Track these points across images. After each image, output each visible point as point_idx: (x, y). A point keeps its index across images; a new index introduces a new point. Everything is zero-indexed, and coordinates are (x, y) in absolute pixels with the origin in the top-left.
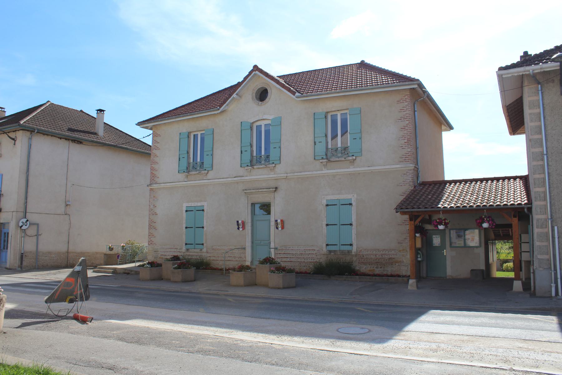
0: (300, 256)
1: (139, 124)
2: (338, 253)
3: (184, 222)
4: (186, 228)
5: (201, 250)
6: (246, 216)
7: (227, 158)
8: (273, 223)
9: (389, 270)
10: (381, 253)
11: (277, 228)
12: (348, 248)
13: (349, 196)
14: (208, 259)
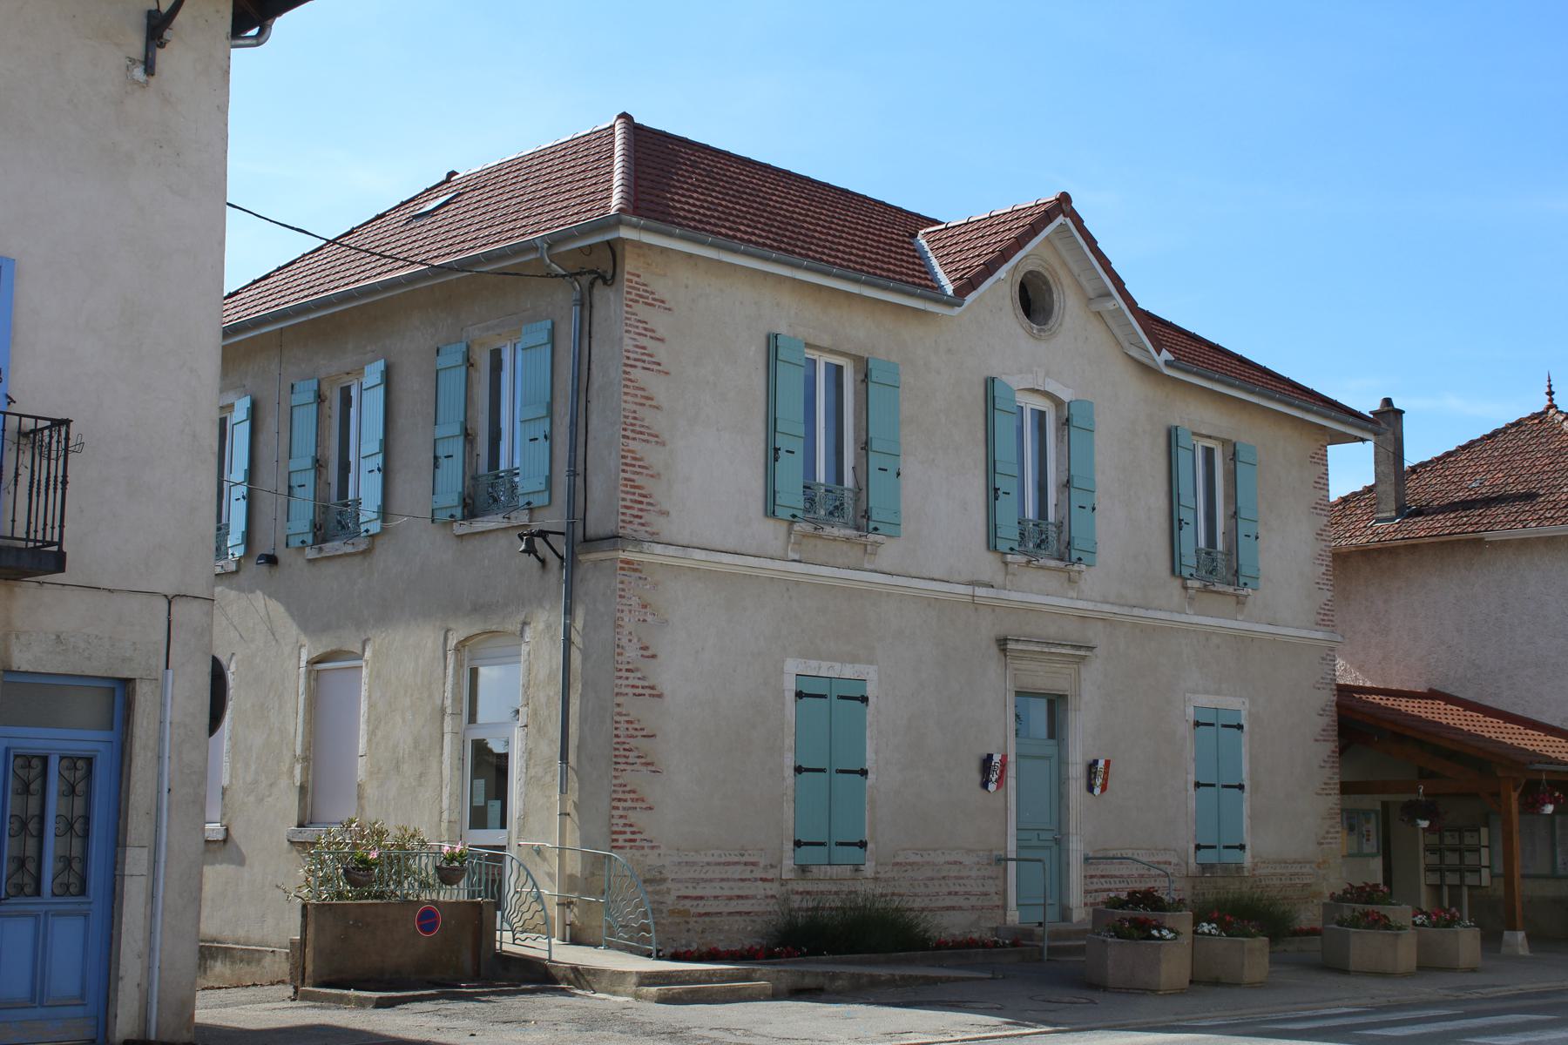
3: (789, 741)
5: (857, 868)
7: (940, 499)
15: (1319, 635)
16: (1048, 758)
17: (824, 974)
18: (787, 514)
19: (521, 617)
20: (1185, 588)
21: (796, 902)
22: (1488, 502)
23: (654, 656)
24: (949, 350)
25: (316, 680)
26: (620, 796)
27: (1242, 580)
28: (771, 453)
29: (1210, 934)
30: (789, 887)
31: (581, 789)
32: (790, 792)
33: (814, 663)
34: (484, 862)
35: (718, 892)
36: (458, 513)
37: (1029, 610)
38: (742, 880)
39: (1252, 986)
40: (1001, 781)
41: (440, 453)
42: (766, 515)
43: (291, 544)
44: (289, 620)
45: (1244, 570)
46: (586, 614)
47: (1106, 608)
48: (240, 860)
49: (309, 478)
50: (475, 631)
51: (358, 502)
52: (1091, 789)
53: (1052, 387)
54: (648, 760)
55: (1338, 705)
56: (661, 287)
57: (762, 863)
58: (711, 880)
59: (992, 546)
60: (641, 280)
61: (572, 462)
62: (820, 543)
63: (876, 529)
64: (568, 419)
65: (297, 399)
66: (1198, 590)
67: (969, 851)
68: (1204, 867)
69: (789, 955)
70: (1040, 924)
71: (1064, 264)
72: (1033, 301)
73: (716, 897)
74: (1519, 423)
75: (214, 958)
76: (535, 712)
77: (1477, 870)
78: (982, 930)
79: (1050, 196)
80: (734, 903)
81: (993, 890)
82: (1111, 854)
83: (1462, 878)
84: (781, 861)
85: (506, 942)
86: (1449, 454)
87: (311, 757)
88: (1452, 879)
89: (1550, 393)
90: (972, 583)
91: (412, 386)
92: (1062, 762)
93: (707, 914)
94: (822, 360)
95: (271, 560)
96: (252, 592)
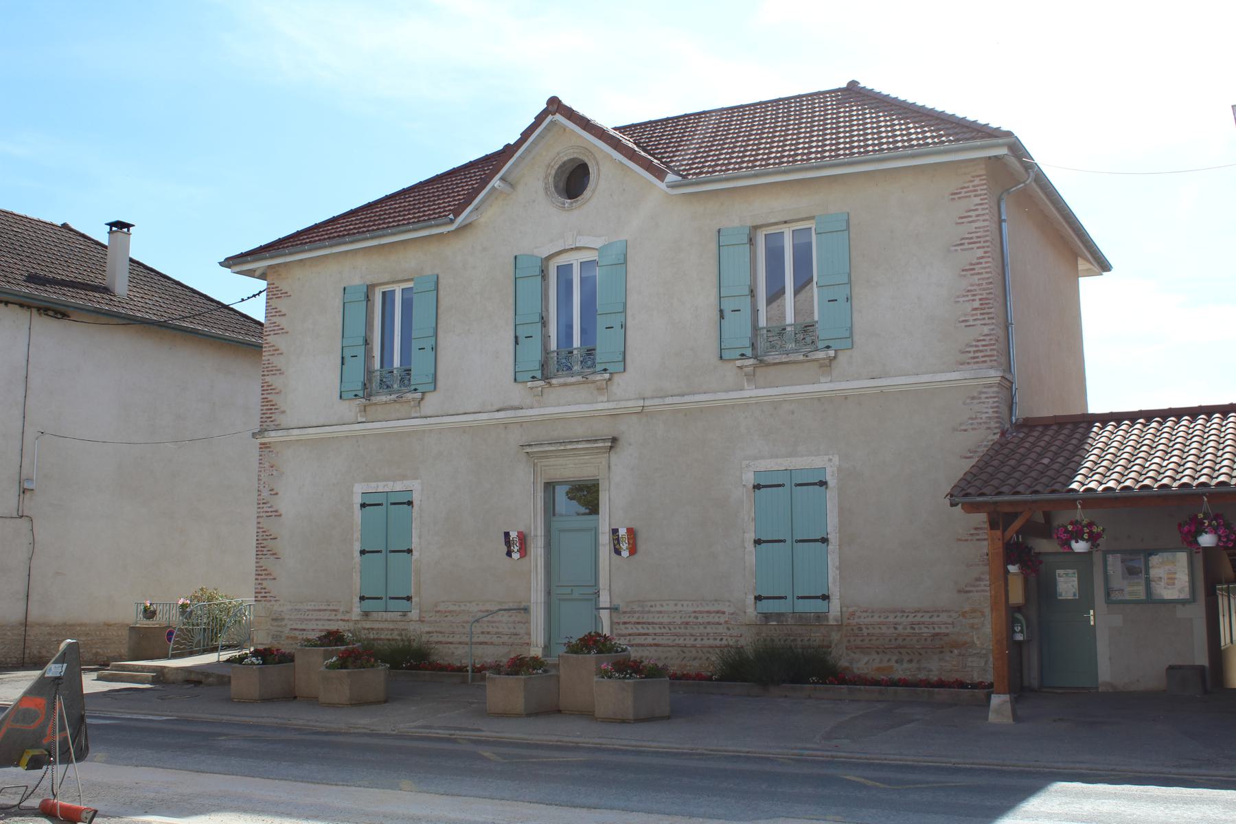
0: (682, 631)
1: (229, 263)
2: (790, 621)
3: (357, 535)
4: (363, 552)
5: (405, 614)
6: (527, 515)
8: (605, 538)
9: (934, 668)
10: (911, 619)
11: (618, 552)
12: (819, 606)
13: (817, 462)
14: (425, 638)
32: (358, 566)
33: (373, 484)
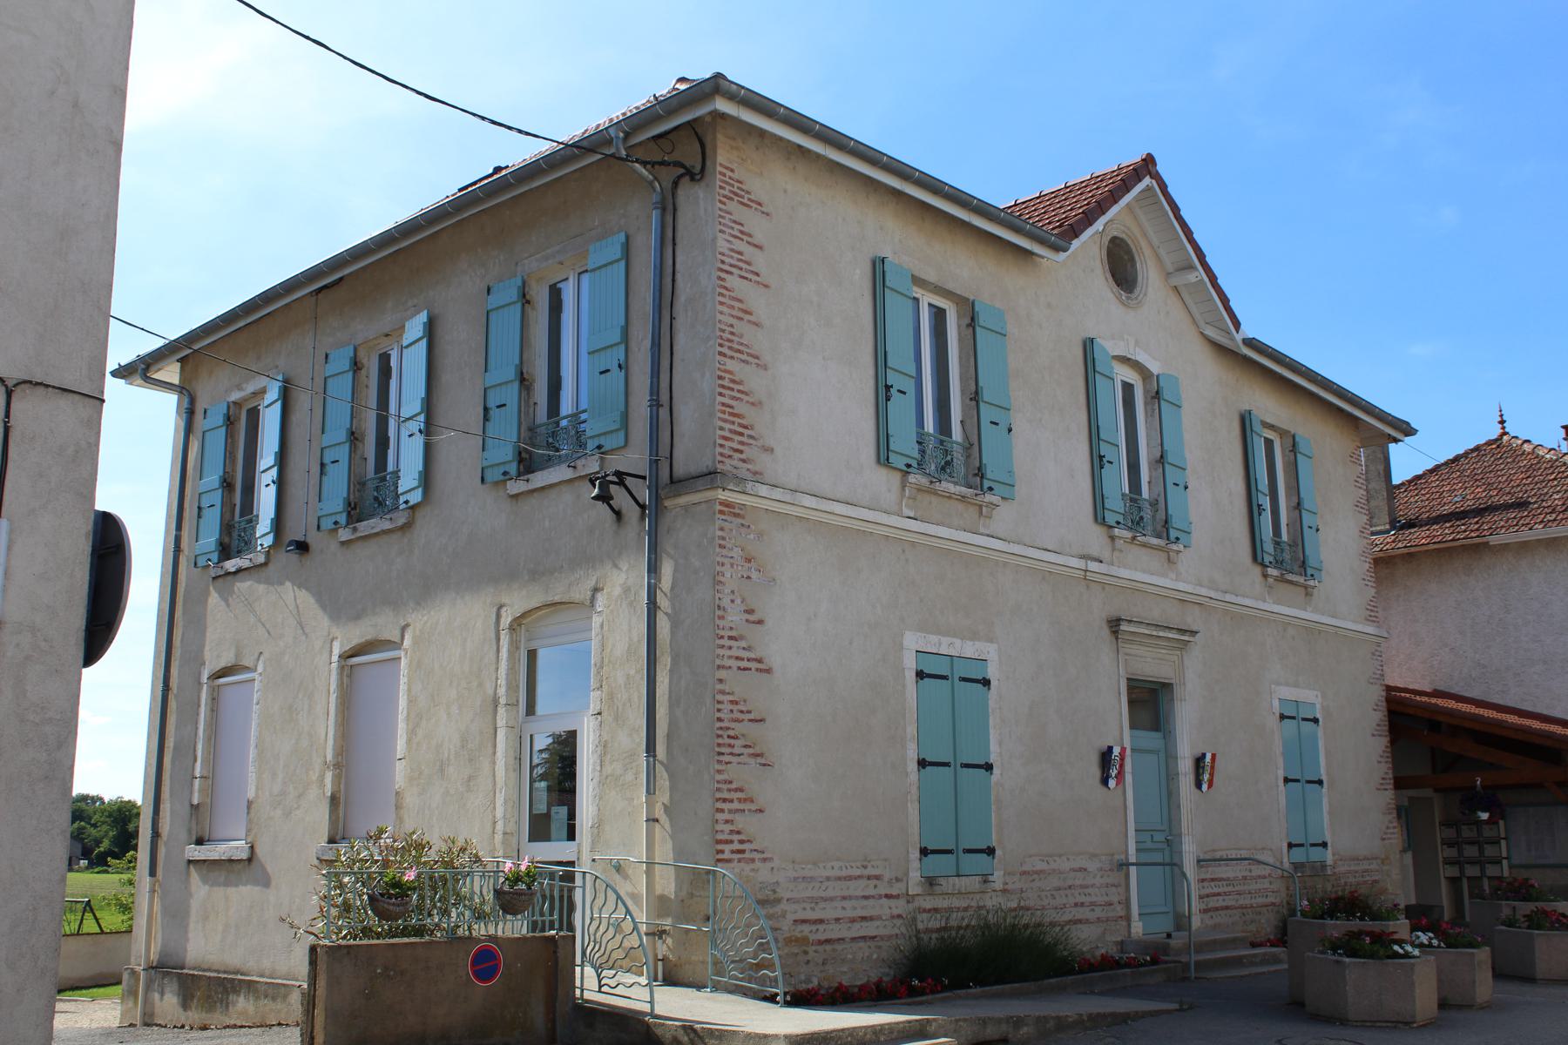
3: (911, 730)
6: (1113, 723)
15: (1370, 629)
16: (1156, 752)
17: (1008, 1019)
18: (898, 462)
19: (591, 583)
20: (1265, 576)
21: (924, 922)
22: (1480, 512)
23: (760, 622)
24: (1049, 305)
25: (350, 676)
26: (726, 795)
27: (1310, 571)
28: (882, 391)
29: (1430, 945)
30: (916, 904)
31: (672, 789)
32: (914, 790)
33: (934, 638)
34: (557, 883)
35: (840, 914)
36: (513, 469)
37: (1135, 589)
38: (866, 898)
39: (1486, 1007)
40: (1120, 776)
41: (491, 404)
42: (878, 461)
43: (323, 526)
44: (320, 613)
45: (1311, 562)
46: (676, 571)
47: (1204, 591)
48: (265, 881)
49: (343, 453)
50: (534, 603)
51: (396, 474)
52: (1199, 785)
53: (1142, 357)
54: (758, 750)
55: (1389, 700)
56: (757, 187)
57: (887, 875)
58: (832, 899)
59: (1099, 517)
60: (735, 176)
61: (655, 390)
62: (933, 499)
63: (991, 489)
64: (648, 343)
65: (331, 369)
66: (1276, 579)
67: (1093, 856)
68: (1297, 866)
69: (932, 992)
70: (1169, 936)
71: (1145, 235)
72: (1121, 267)
73: (837, 920)
74: (1477, 448)
75: (236, 992)
76: (611, 697)
77: (1497, 862)
78: (1108, 948)
79: (1134, 157)
80: (857, 925)
81: (1115, 899)
82: (1218, 855)
83: (1483, 870)
84: (907, 874)
85: (589, 985)
86: (1418, 478)
87: (343, 764)
88: (1472, 871)
89: (1502, 422)
90: (1083, 557)
91: (460, 336)
92: (1170, 756)
93: (828, 941)
94: (926, 299)
95: (302, 547)
96: (282, 584)
